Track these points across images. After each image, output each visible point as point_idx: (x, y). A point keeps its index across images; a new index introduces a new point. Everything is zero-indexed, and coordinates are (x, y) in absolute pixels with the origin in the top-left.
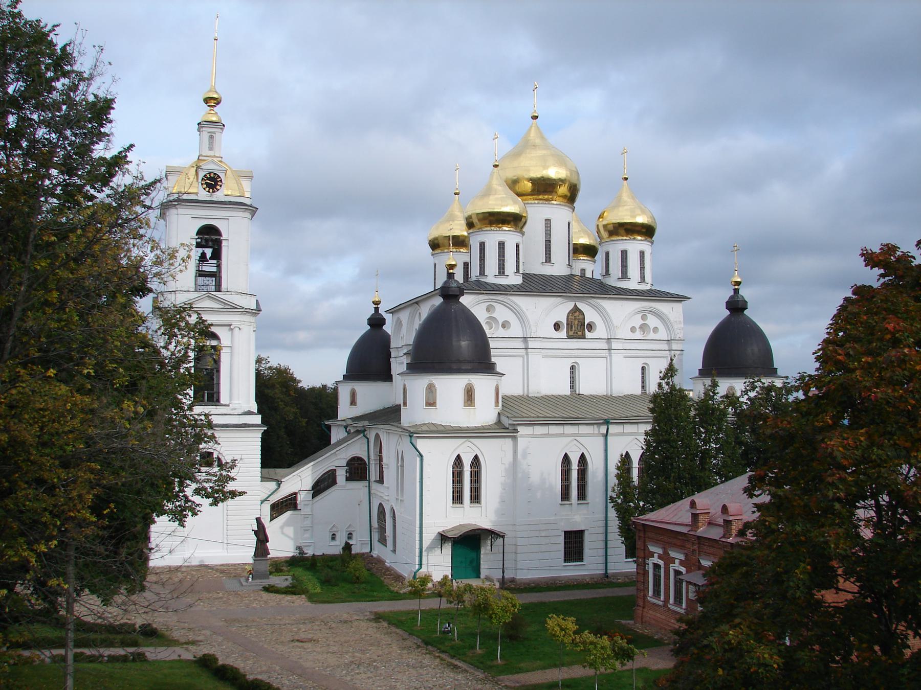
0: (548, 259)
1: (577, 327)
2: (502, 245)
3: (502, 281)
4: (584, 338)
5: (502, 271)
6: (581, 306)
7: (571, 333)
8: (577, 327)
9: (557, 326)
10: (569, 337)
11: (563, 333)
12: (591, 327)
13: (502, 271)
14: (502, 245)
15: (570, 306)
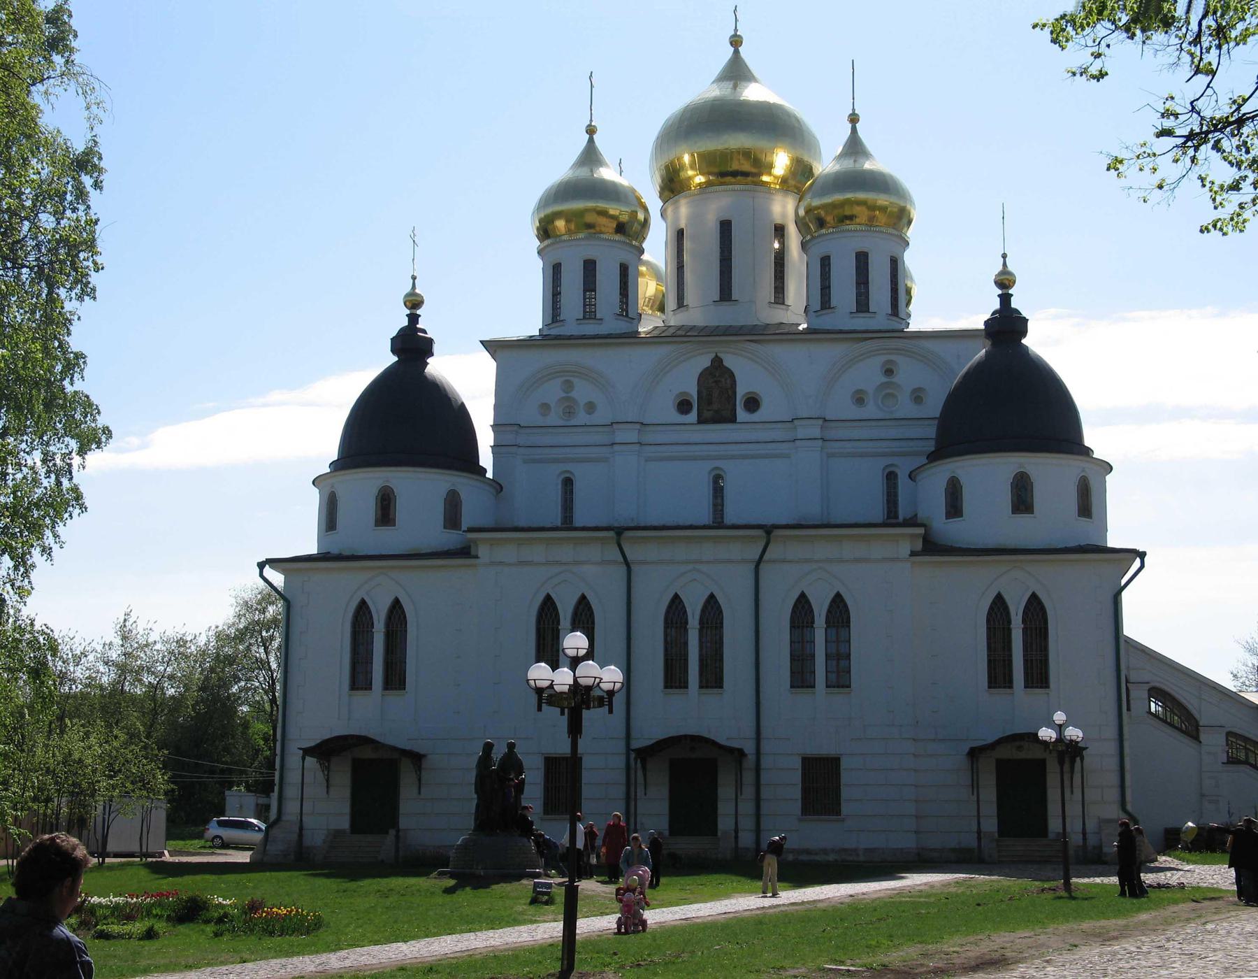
0: (725, 293)
1: (717, 399)
2: (590, 267)
3: (590, 328)
4: (733, 419)
5: (589, 313)
6: (730, 361)
7: (707, 414)
8: (717, 399)
9: (684, 406)
10: (701, 421)
11: (693, 416)
12: (753, 403)
13: (589, 313)
14: (590, 267)
15: (704, 362)
